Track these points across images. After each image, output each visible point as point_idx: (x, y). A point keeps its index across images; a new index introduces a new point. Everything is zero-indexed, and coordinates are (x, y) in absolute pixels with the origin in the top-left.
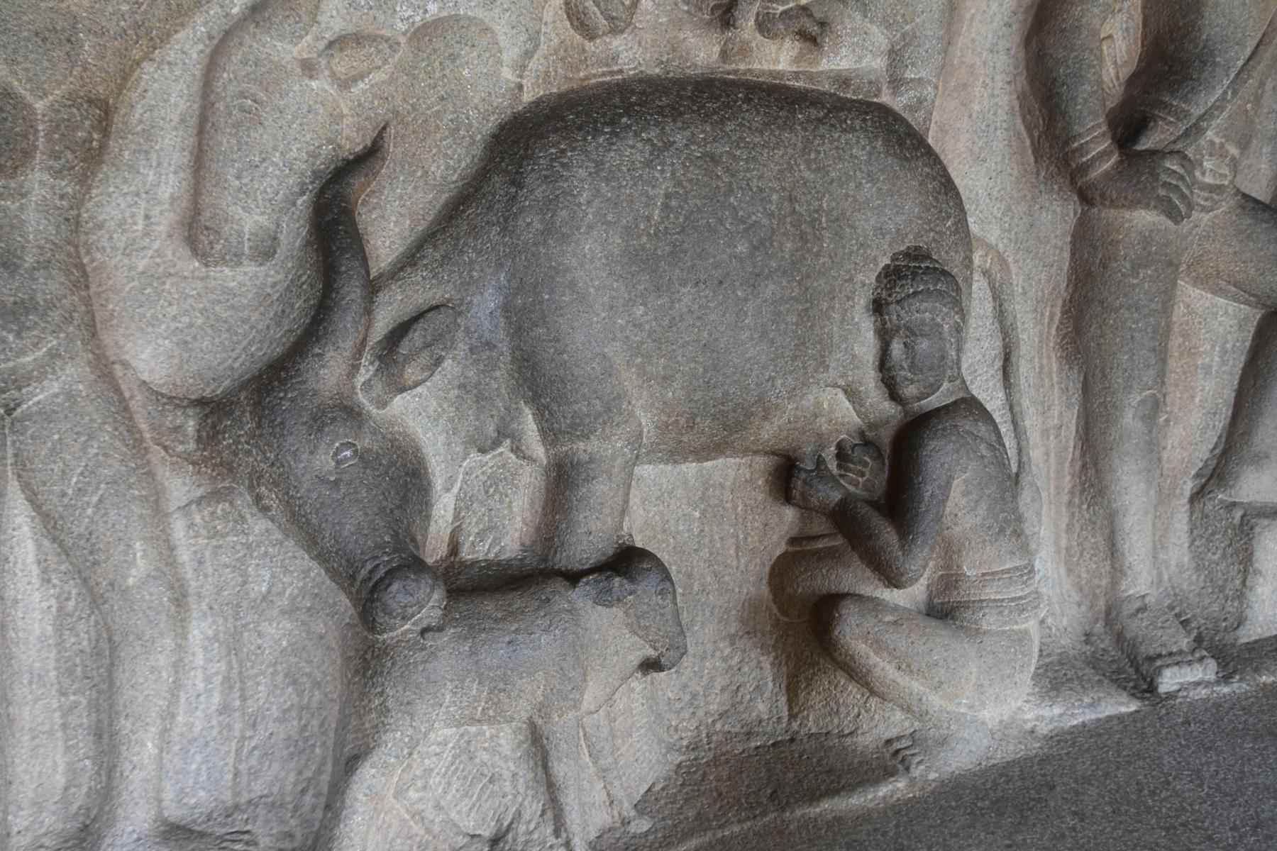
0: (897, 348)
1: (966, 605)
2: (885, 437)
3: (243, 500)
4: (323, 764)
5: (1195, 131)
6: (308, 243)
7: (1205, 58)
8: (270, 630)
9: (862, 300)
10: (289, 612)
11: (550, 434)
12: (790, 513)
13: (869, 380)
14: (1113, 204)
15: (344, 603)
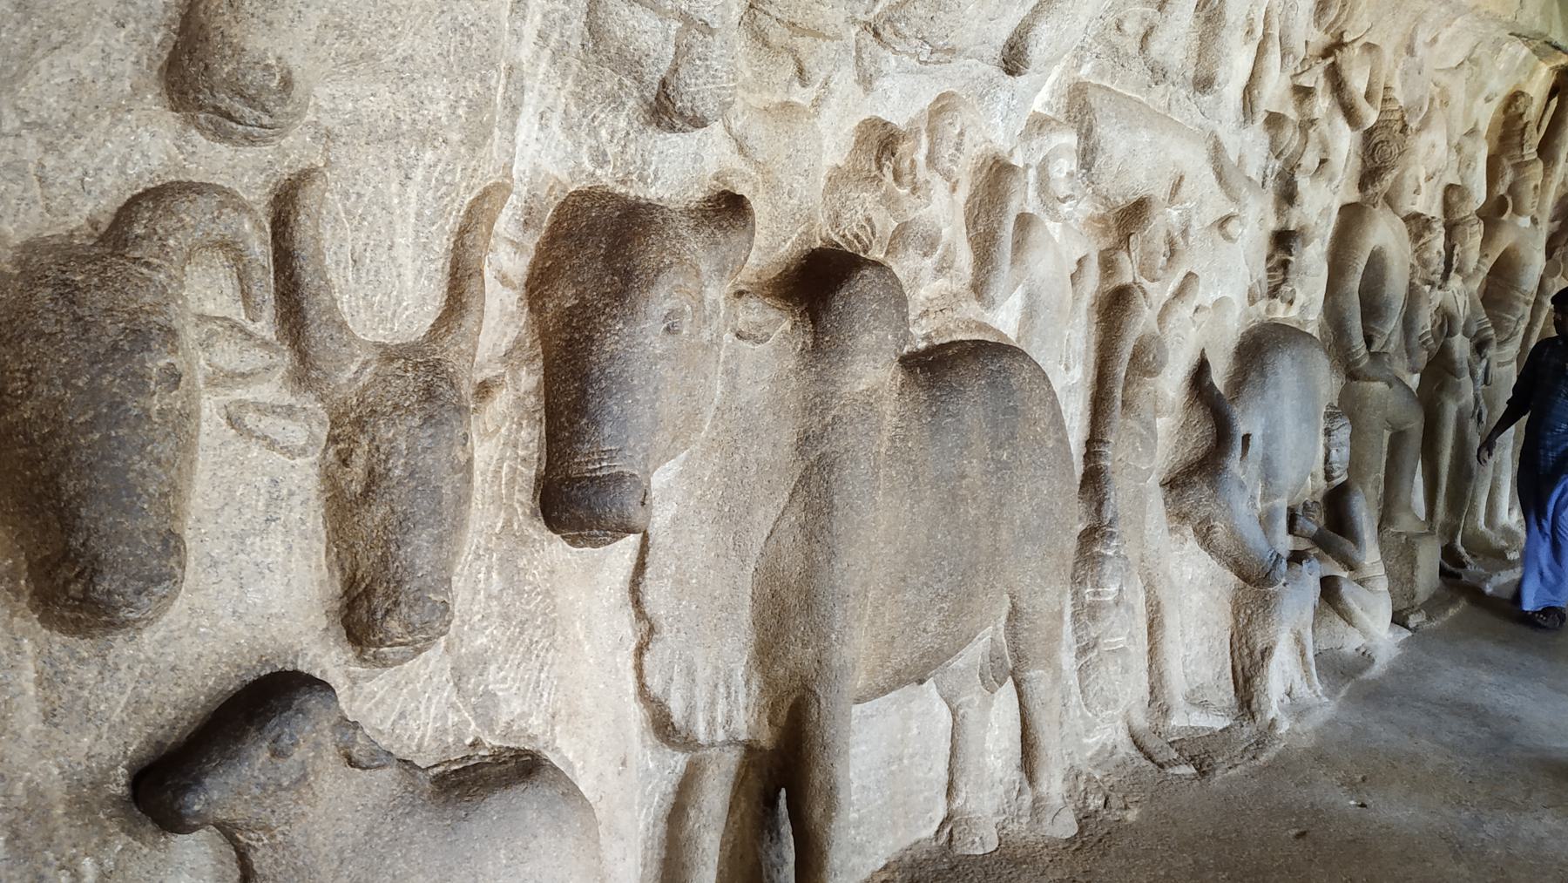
0: (1334, 452)
1: (1368, 579)
2: (1319, 498)
3: (1188, 530)
4: (1225, 662)
5: (1387, 343)
6: (1190, 406)
7: (1387, 304)
8: (1195, 597)
9: (1321, 430)
10: (1202, 588)
11: (1265, 497)
12: (1290, 538)
13: (1321, 466)
14: (1369, 379)
15: (1231, 578)
